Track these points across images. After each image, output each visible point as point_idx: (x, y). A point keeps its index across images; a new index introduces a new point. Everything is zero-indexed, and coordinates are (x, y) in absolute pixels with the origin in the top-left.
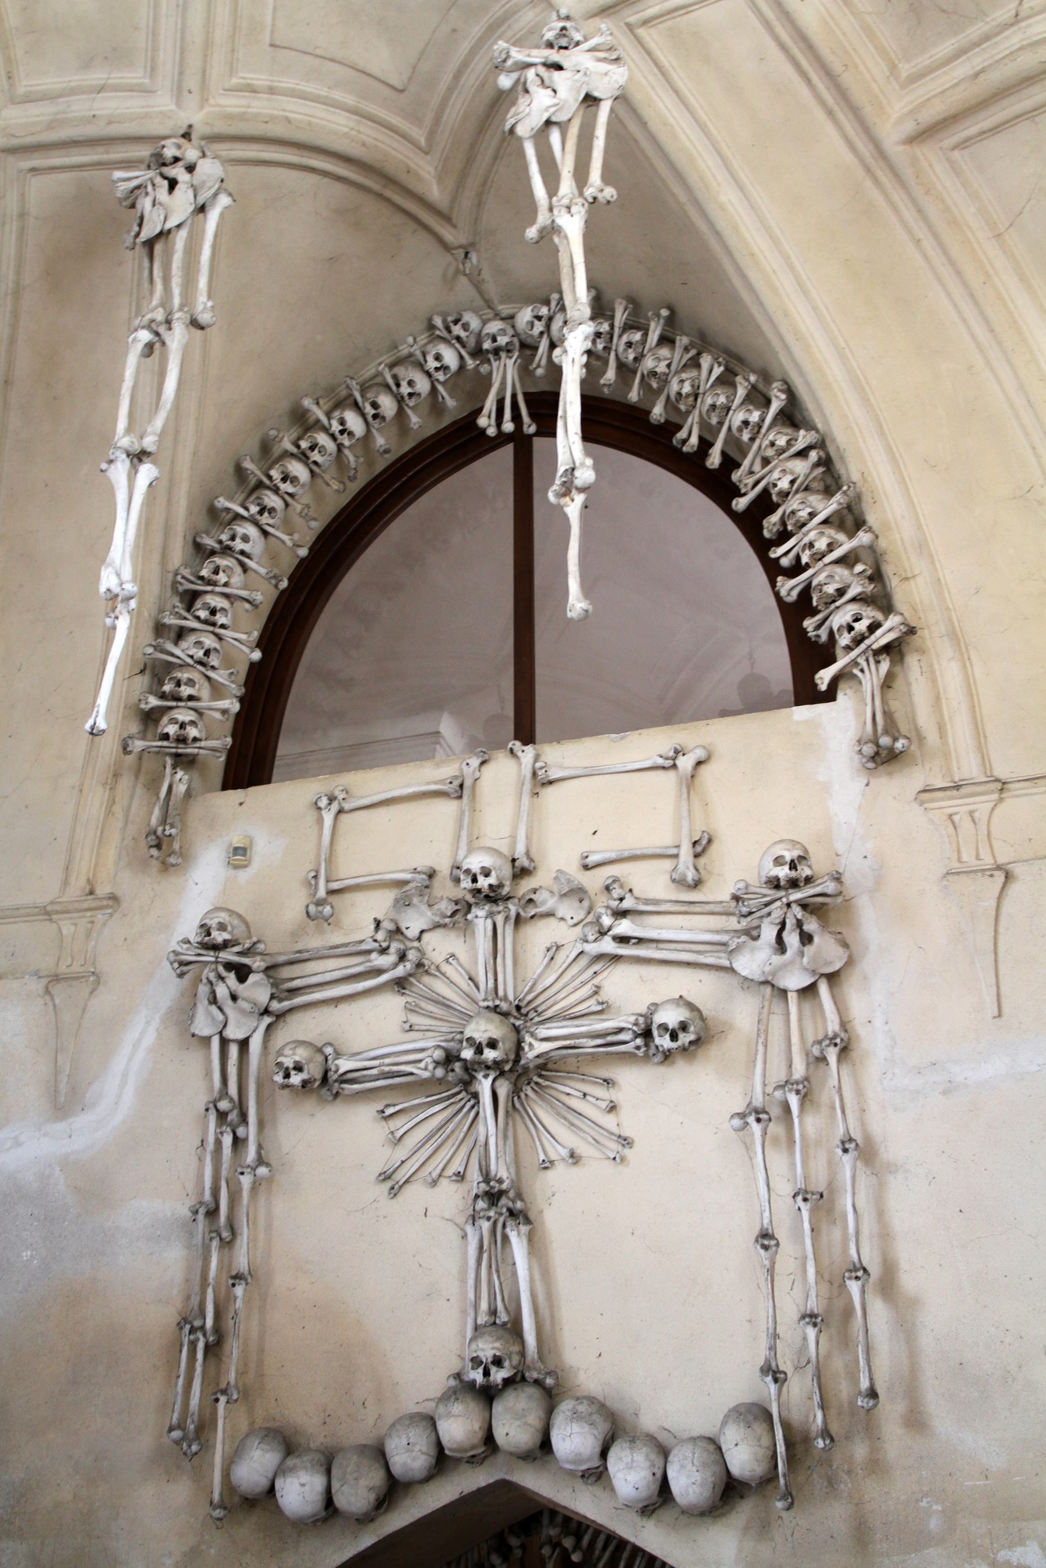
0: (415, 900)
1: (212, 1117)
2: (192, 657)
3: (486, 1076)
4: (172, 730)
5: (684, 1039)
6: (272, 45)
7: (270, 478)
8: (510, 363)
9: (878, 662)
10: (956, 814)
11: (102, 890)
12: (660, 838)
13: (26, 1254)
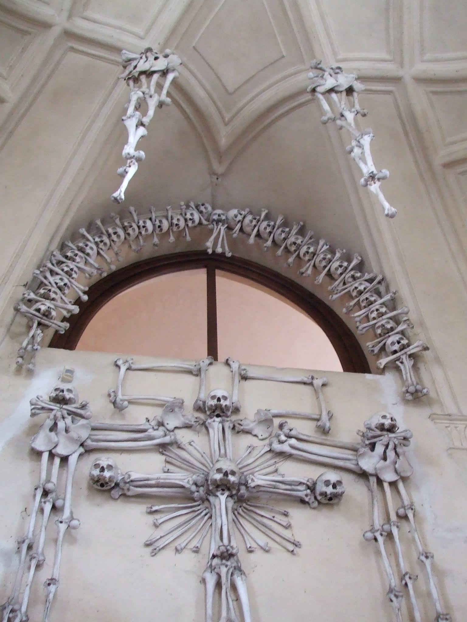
0: (176, 409)
1: (39, 493)
2: (56, 284)
3: (223, 494)
4: (43, 308)
5: (339, 490)
6: (194, 47)
8: (223, 229)
12: (308, 409)
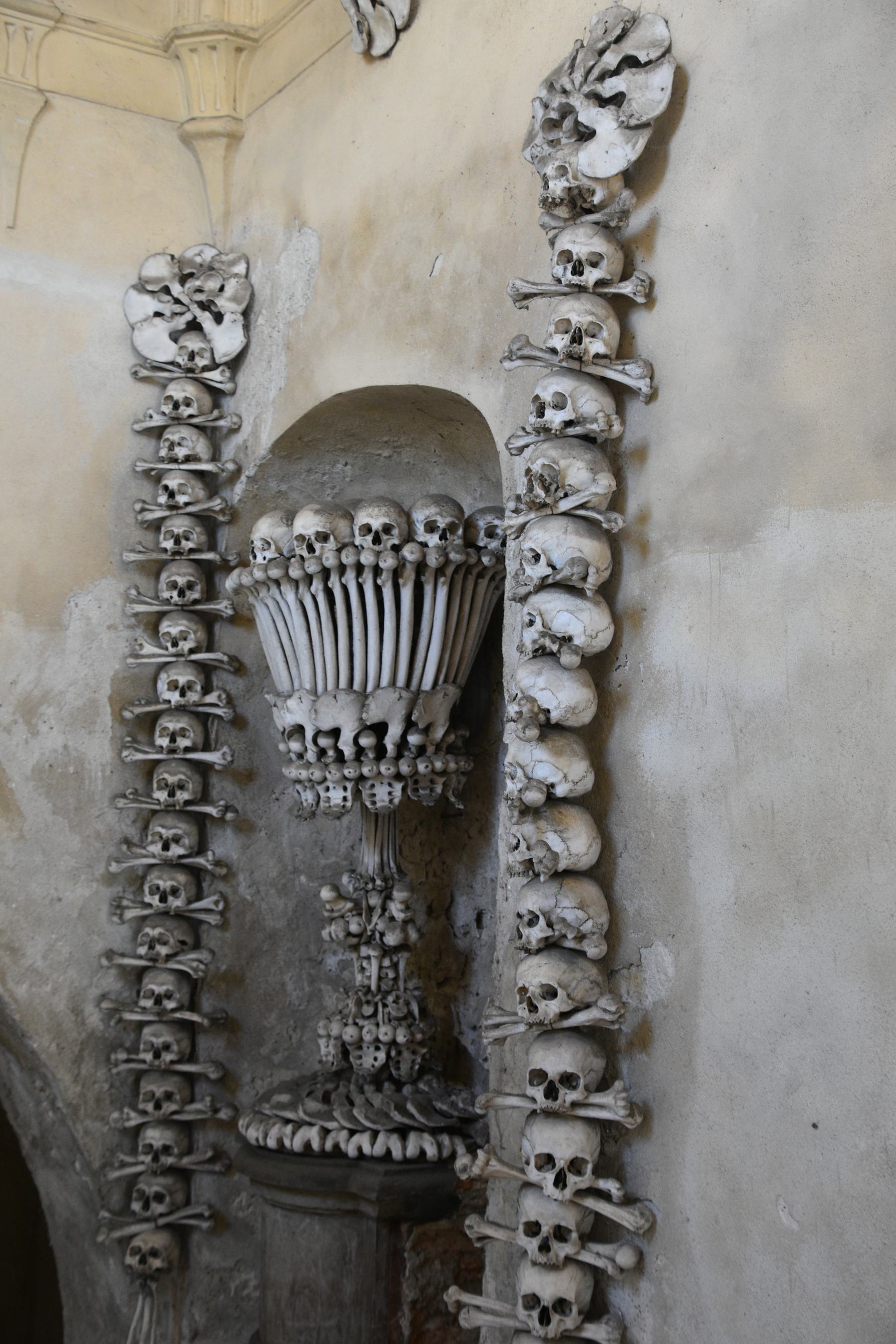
10: (12, 24)
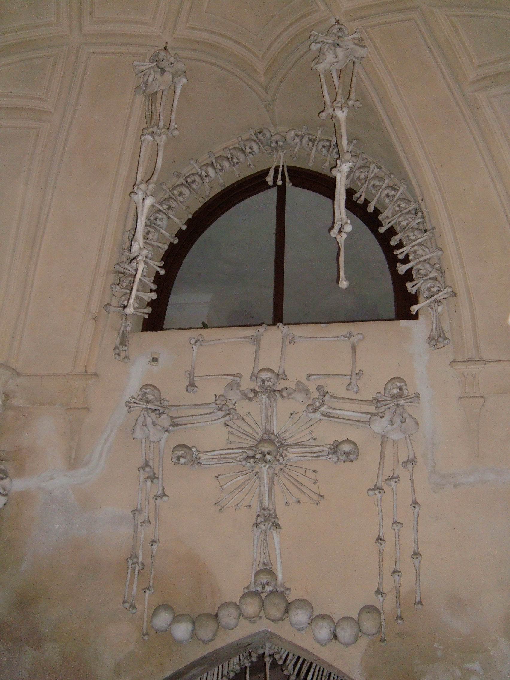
5: (352, 457)
7: (173, 194)
9: (438, 306)
11: (91, 370)
13: (57, 526)
